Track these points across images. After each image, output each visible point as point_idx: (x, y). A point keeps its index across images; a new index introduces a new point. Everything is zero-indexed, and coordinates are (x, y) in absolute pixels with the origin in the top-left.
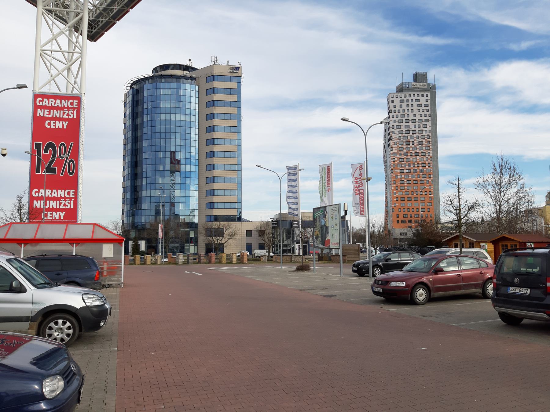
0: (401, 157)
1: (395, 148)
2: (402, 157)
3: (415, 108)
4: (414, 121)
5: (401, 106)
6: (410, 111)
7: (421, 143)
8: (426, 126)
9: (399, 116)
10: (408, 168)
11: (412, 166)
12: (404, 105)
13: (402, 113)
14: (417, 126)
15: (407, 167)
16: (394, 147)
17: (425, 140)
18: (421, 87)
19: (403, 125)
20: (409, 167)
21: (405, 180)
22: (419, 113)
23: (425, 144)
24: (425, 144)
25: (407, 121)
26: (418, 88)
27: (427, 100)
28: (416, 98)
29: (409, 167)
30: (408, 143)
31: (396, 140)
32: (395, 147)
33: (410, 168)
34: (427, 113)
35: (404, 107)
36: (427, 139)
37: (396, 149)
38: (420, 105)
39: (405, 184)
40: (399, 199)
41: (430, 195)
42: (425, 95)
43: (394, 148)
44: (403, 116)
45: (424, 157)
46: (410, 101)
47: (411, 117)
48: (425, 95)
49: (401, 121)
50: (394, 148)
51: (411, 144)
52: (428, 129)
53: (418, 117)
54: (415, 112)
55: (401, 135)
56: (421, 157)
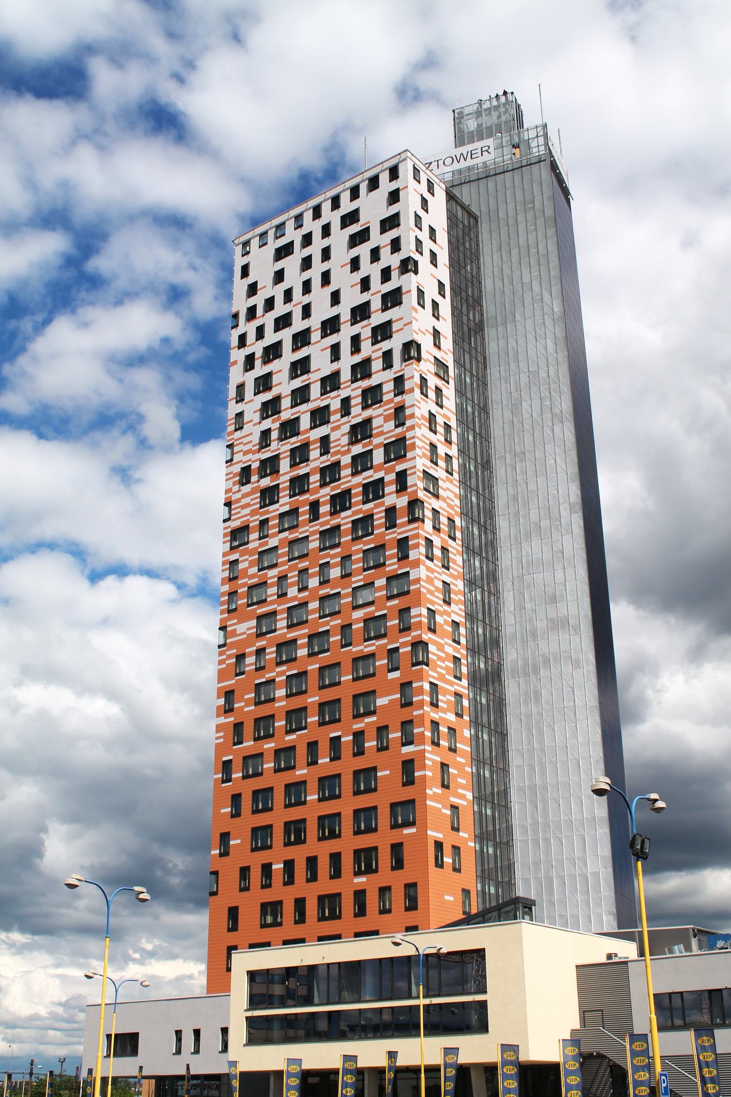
0: (267, 543)
1: (244, 501)
2: (273, 542)
4: (331, 326)
5: (279, 276)
7: (360, 432)
10: (294, 598)
11: (314, 582)
13: (280, 309)
15: (292, 592)
16: (239, 495)
17: (380, 411)
19: (281, 367)
20: (300, 590)
21: (280, 674)
22: (358, 276)
23: (381, 433)
24: (381, 433)
25: (302, 339)
28: (347, 206)
29: (300, 590)
30: (300, 454)
31: (250, 456)
32: (245, 496)
33: (306, 593)
35: (294, 278)
36: (391, 401)
37: (248, 505)
38: (358, 239)
39: (281, 699)
40: (247, 803)
41: (406, 749)
43: (238, 500)
45: (376, 506)
47: (322, 311)
49: (273, 352)
50: (238, 500)
51: (314, 454)
53: (352, 298)
55: (273, 422)
56: (360, 511)
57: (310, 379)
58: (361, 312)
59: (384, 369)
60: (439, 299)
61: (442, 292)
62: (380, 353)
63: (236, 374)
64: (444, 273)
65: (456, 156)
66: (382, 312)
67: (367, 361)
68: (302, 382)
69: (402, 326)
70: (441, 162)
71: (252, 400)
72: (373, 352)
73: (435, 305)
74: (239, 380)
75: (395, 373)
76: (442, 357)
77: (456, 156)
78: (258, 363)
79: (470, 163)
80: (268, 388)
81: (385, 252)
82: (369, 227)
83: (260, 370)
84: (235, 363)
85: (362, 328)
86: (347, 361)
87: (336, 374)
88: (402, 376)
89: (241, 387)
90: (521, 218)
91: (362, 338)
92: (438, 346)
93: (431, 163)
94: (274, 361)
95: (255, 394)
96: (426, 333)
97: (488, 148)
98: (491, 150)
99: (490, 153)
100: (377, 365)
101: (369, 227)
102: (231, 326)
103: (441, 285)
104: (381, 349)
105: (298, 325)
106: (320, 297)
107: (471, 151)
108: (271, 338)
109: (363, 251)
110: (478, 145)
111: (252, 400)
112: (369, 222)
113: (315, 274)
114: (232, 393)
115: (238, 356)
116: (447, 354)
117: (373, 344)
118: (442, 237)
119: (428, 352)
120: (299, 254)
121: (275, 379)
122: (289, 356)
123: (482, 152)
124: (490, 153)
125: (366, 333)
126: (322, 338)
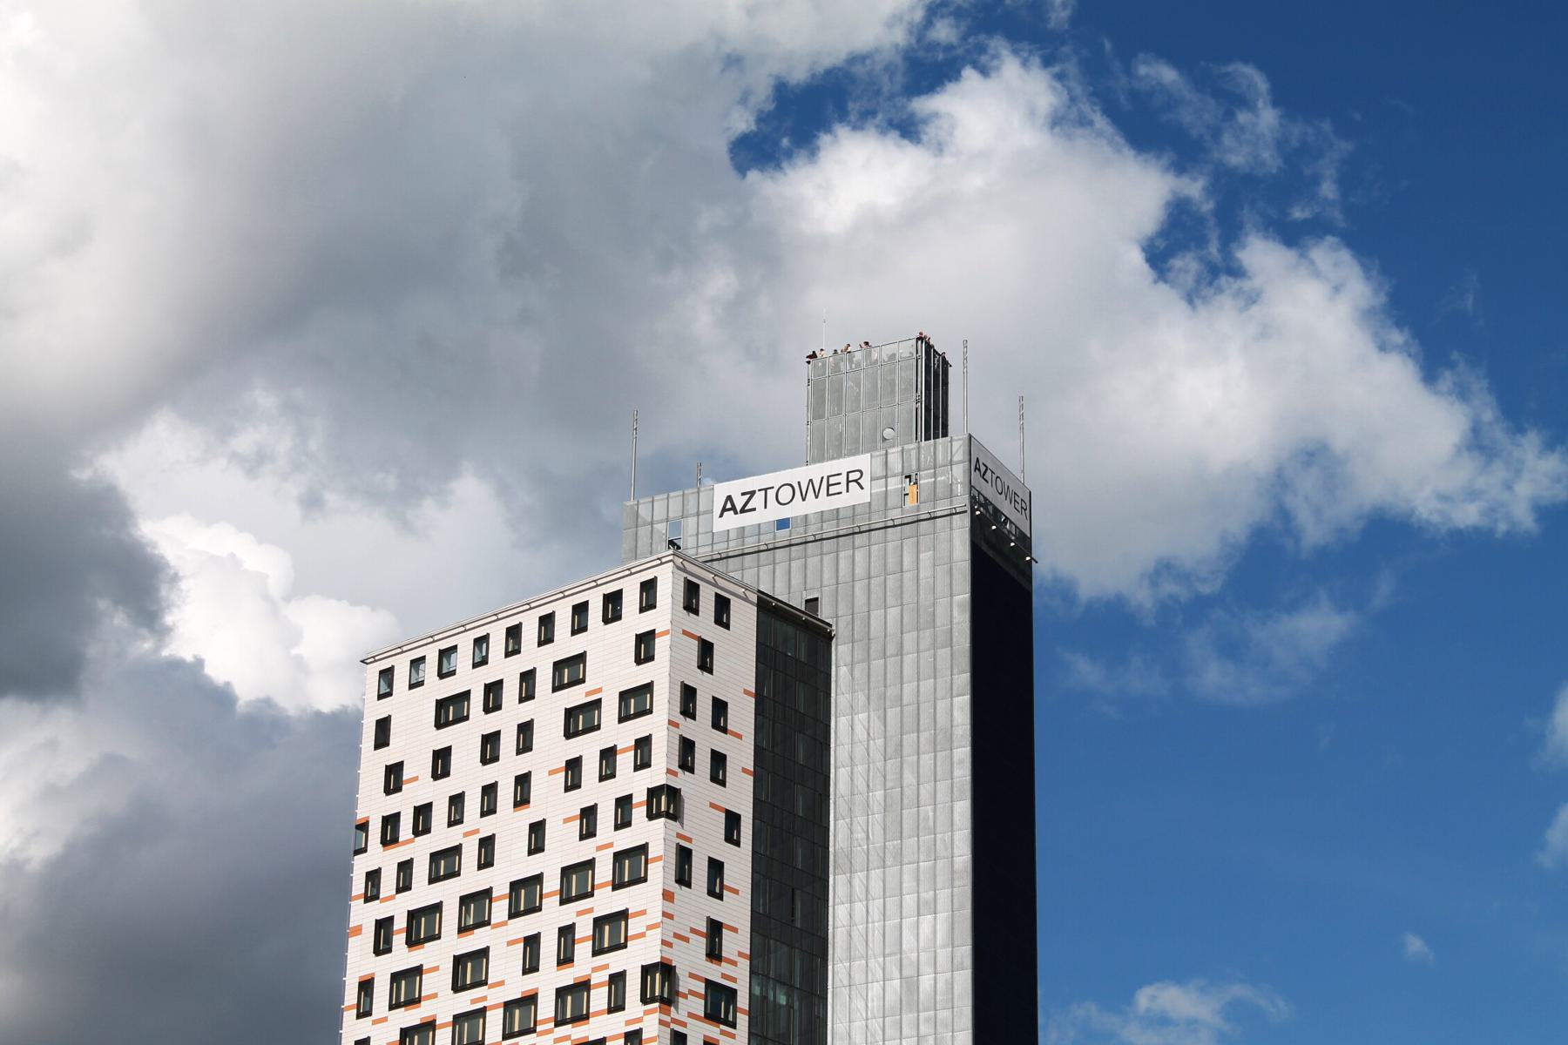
3: (552, 747)
4: (525, 895)
5: (441, 762)
6: (506, 794)
8: (611, 932)
9: (421, 871)
12: (464, 739)
13: (441, 836)
14: (549, 949)
18: (812, 506)
25: (476, 905)
26: (783, 524)
27: (645, 646)
28: (565, 644)
34: (636, 784)
35: (468, 775)
38: (579, 720)
42: (631, 600)
44: (445, 864)
46: (511, 691)
47: (513, 863)
48: (631, 600)
49: (422, 926)
52: (631, 960)
53: (564, 847)
54: (551, 801)
57: (484, 998)
58: (577, 880)
59: (610, 1011)
60: (724, 852)
61: (732, 835)
62: (603, 977)
63: (360, 960)
64: (740, 794)
65: (799, 483)
66: (614, 889)
67: (583, 986)
68: (474, 1001)
69: (644, 930)
70: (771, 494)
71: (385, 1019)
72: (595, 970)
73: (716, 867)
74: (364, 972)
75: (628, 1023)
76: (724, 976)
77: (799, 483)
78: (399, 940)
79: (825, 503)
80: (413, 1001)
81: (625, 761)
82: (599, 701)
83: (402, 957)
84: (358, 930)
85: (579, 914)
86: (550, 979)
87: (530, 1000)
88: (639, 1032)
89: (366, 986)
90: (909, 639)
91: (635, 801)
92: (714, 954)
93: (752, 493)
94: (426, 945)
95: (391, 1008)
96: (692, 936)
97: (858, 474)
98: (865, 481)
99: (862, 488)
100: (599, 998)
101: (599, 701)
102: (353, 850)
103: (733, 820)
104: (606, 967)
105: (471, 879)
106: (510, 826)
107: (828, 477)
108: (422, 893)
109: (588, 748)
110: (843, 465)
111: (385, 1019)
112: (599, 690)
113: (504, 773)
114: (351, 996)
115: (363, 915)
116: (734, 963)
117: (595, 954)
118: (743, 715)
119: (692, 976)
120: (479, 722)
121: (429, 984)
122: (451, 944)
123: (848, 482)
124: (862, 488)
125: (584, 929)
126: (511, 916)
